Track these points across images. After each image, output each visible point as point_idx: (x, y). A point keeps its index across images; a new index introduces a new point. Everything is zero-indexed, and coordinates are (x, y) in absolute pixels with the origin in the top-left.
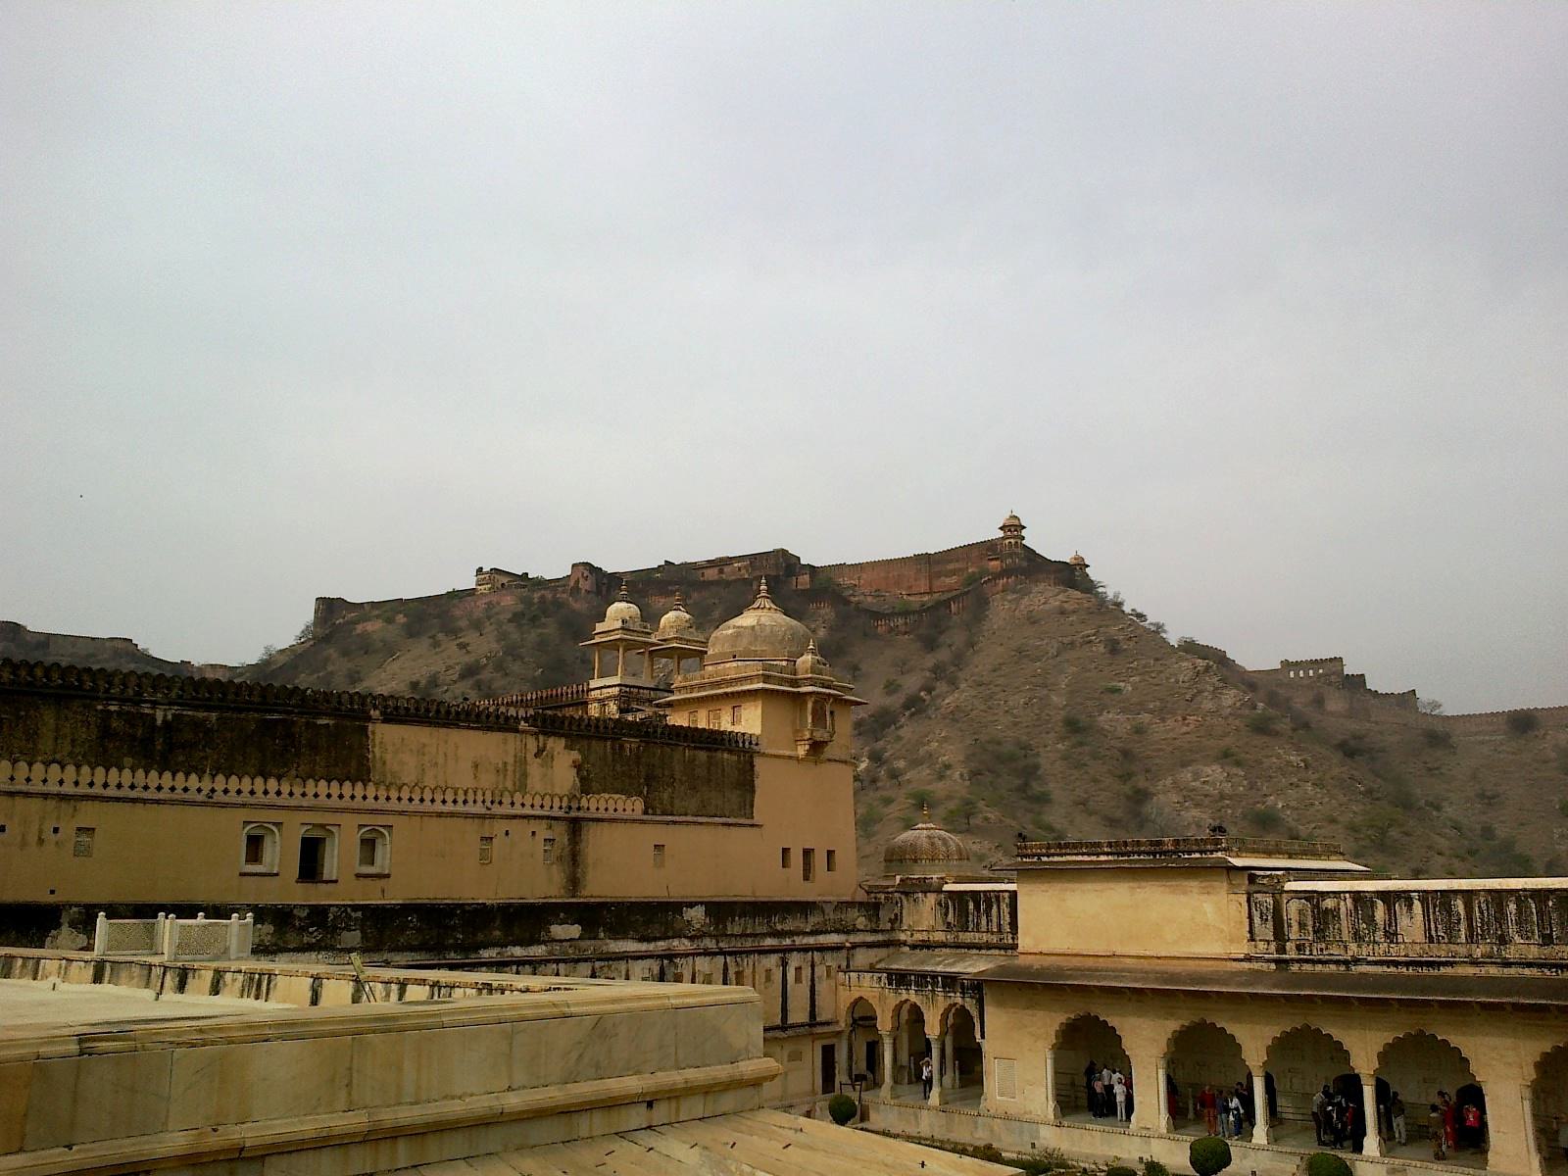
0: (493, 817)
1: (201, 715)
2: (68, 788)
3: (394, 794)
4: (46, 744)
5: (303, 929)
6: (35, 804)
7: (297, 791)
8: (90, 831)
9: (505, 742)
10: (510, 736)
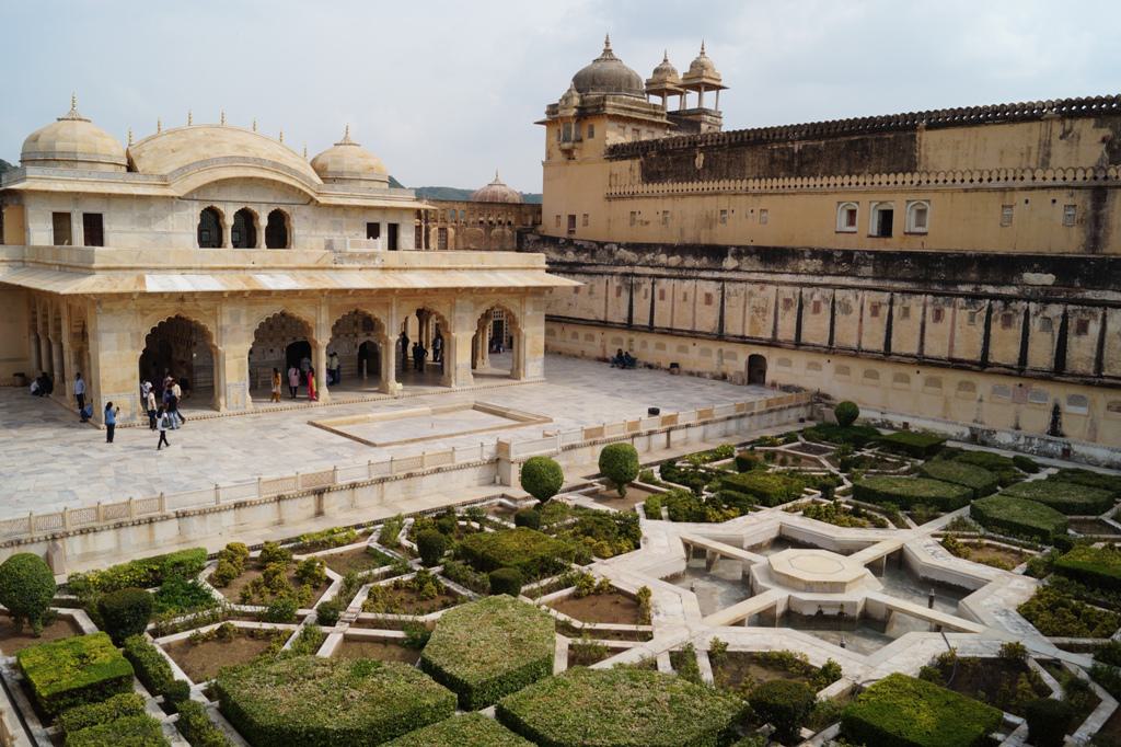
0: (1012, 189)
1: (816, 143)
4: (748, 170)
5: (839, 264)
7: (868, 181)
8: (765, 211)
9: (1030, 130)
10: (1035, 125)
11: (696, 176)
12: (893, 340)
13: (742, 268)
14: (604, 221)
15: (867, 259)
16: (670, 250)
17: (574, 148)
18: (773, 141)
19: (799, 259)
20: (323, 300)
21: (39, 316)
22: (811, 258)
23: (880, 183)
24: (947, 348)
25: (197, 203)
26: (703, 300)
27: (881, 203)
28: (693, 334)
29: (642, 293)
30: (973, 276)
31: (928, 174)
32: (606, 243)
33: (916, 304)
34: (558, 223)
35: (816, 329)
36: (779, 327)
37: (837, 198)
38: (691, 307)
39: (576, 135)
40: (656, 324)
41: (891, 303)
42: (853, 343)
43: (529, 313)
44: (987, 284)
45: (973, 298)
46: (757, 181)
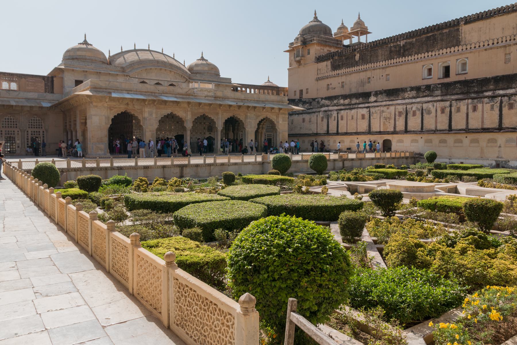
1: (411, 40)
2: (384, 66)
3: (468, 47)
4: (380, 58)
5: (424, 92)
6: (378, 70)
7: (437, 53)
11: (357, 64)
12: (453, 123)
13: (379, 100)
14: (316, 90)
15: (437, 87)
16: (345, 97)
17: (301, 59)
18: (391, 42)
19: (405, 92)
20: (189, 109)
21: (68, 124)
22: (410, 91)
23: (443, 53)
24: (480, 124)
25: (137, 80)
26: (361, 118)
27: (444, 63)
28: (357, 133)
29: (333, 118)
30: (492, 87)
31: (466, 45)
32: (316, 98)
33: (463, 105)
34: (295, 95)
35: (414, 123)
36: (397, 125)
37: (422, 63)
38: (355, 121)
39: (302, 54)
40: (340, 131)
41: (451, 106)
42: (433, 127)
43: (280, 122)
44: (499, 90)
45: (493, 97)
46: (384, 62)
